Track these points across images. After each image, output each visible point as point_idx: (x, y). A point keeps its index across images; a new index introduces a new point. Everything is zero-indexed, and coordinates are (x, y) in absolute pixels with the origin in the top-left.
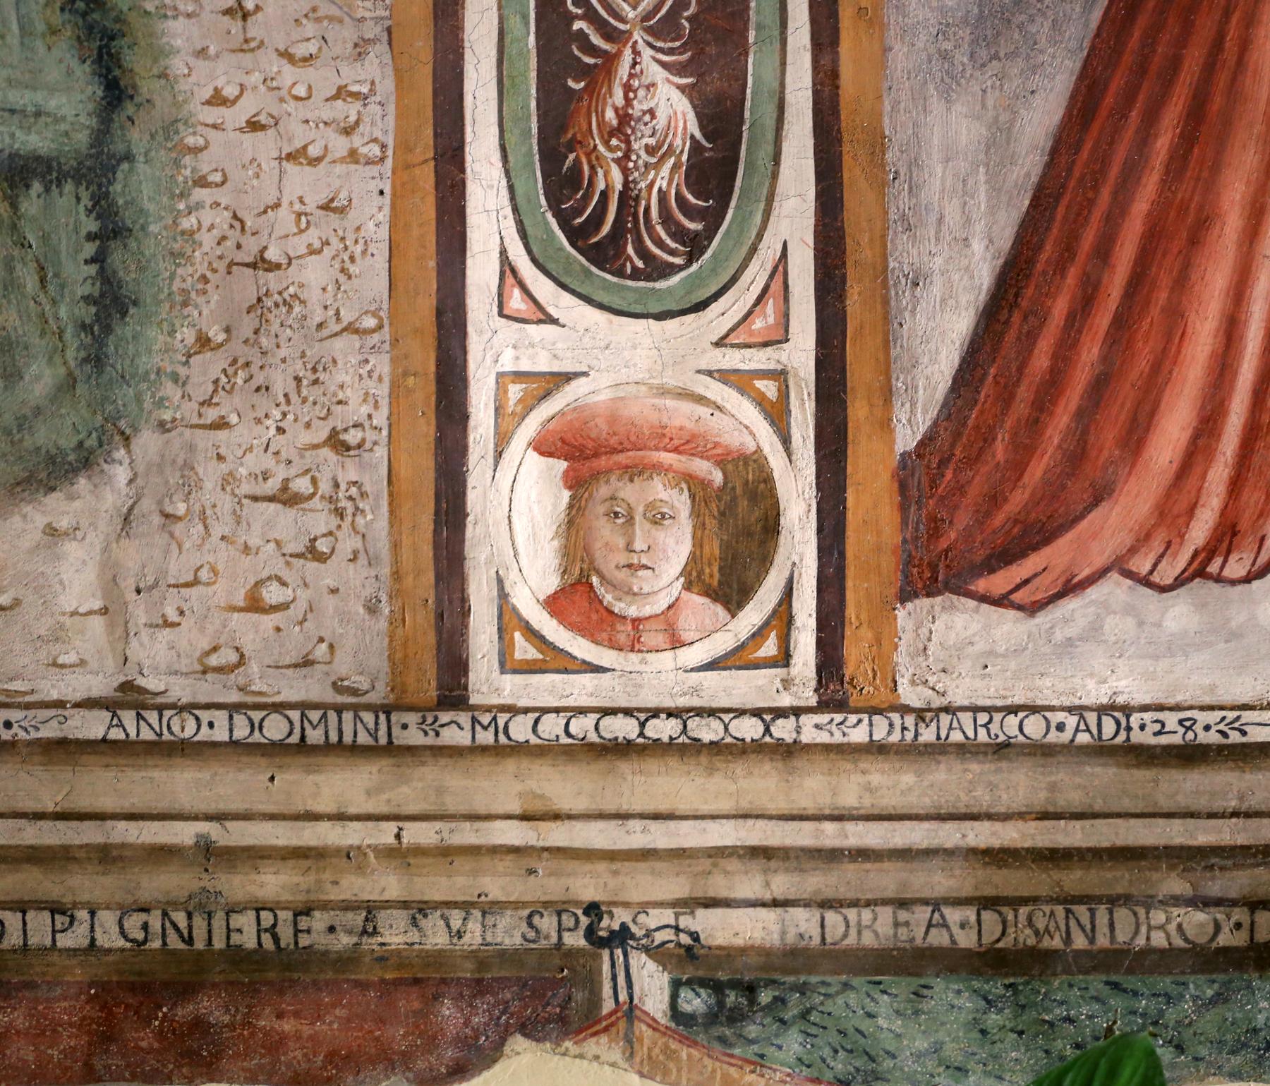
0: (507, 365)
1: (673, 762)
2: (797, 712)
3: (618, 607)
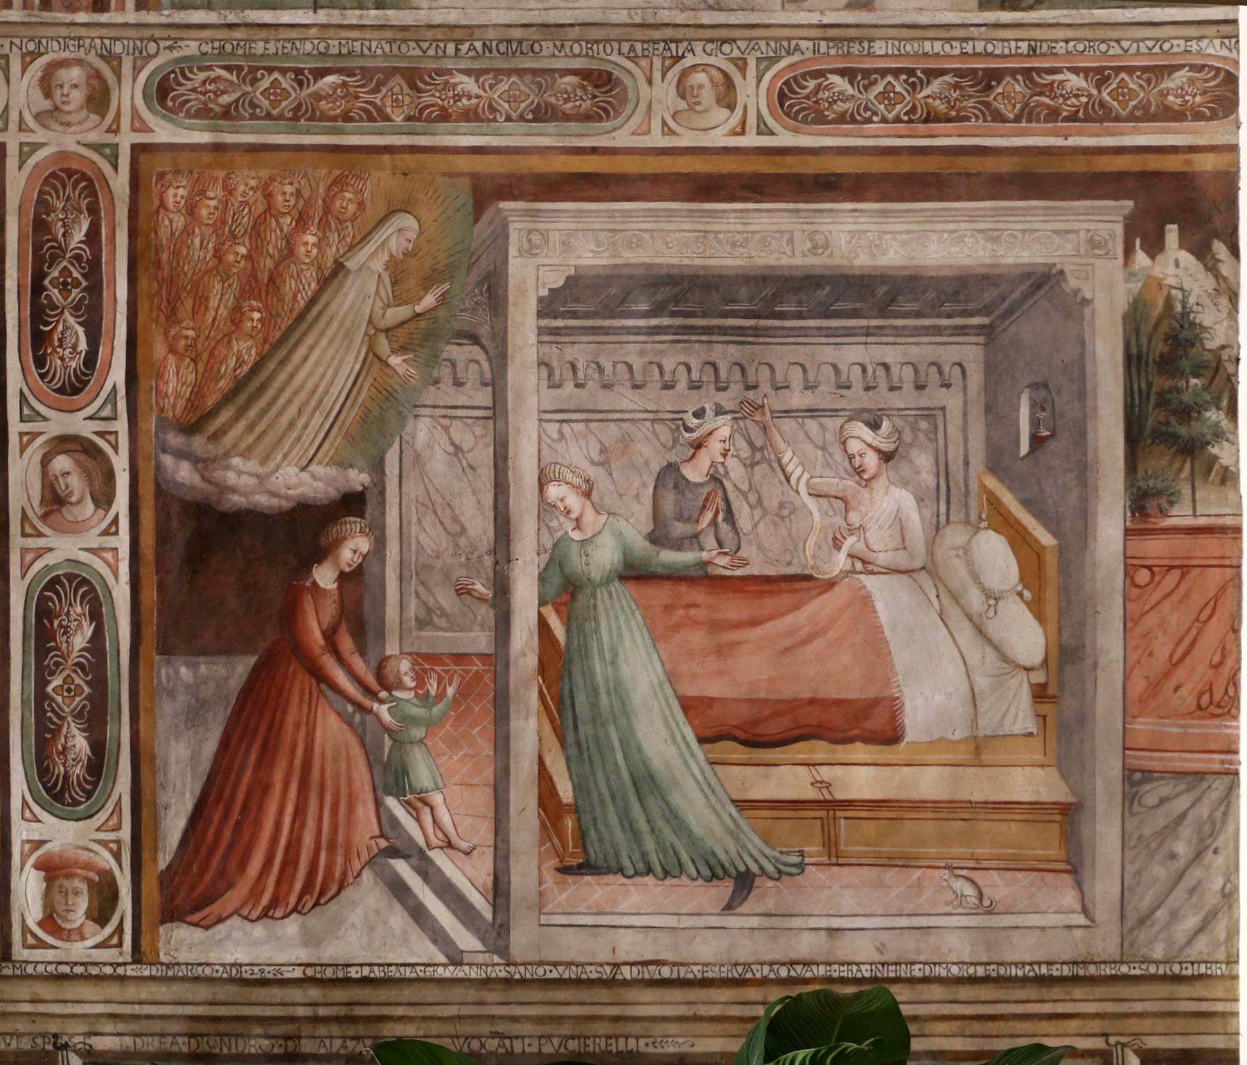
0: (24, 837)
1: (82, 982)
2: (125, 964)
3: (63, 925)
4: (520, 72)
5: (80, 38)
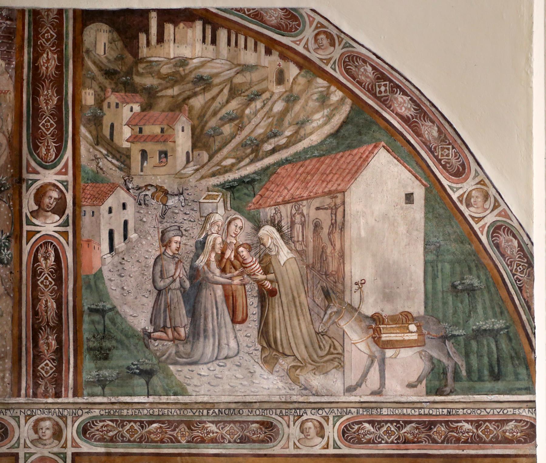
4: (234, 422)
5: (49, 409)
